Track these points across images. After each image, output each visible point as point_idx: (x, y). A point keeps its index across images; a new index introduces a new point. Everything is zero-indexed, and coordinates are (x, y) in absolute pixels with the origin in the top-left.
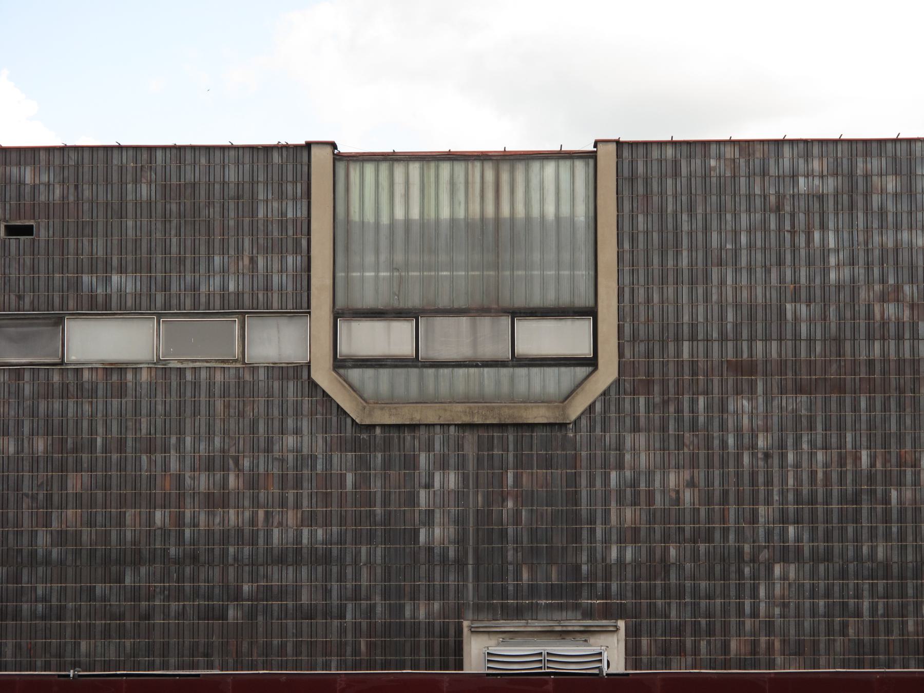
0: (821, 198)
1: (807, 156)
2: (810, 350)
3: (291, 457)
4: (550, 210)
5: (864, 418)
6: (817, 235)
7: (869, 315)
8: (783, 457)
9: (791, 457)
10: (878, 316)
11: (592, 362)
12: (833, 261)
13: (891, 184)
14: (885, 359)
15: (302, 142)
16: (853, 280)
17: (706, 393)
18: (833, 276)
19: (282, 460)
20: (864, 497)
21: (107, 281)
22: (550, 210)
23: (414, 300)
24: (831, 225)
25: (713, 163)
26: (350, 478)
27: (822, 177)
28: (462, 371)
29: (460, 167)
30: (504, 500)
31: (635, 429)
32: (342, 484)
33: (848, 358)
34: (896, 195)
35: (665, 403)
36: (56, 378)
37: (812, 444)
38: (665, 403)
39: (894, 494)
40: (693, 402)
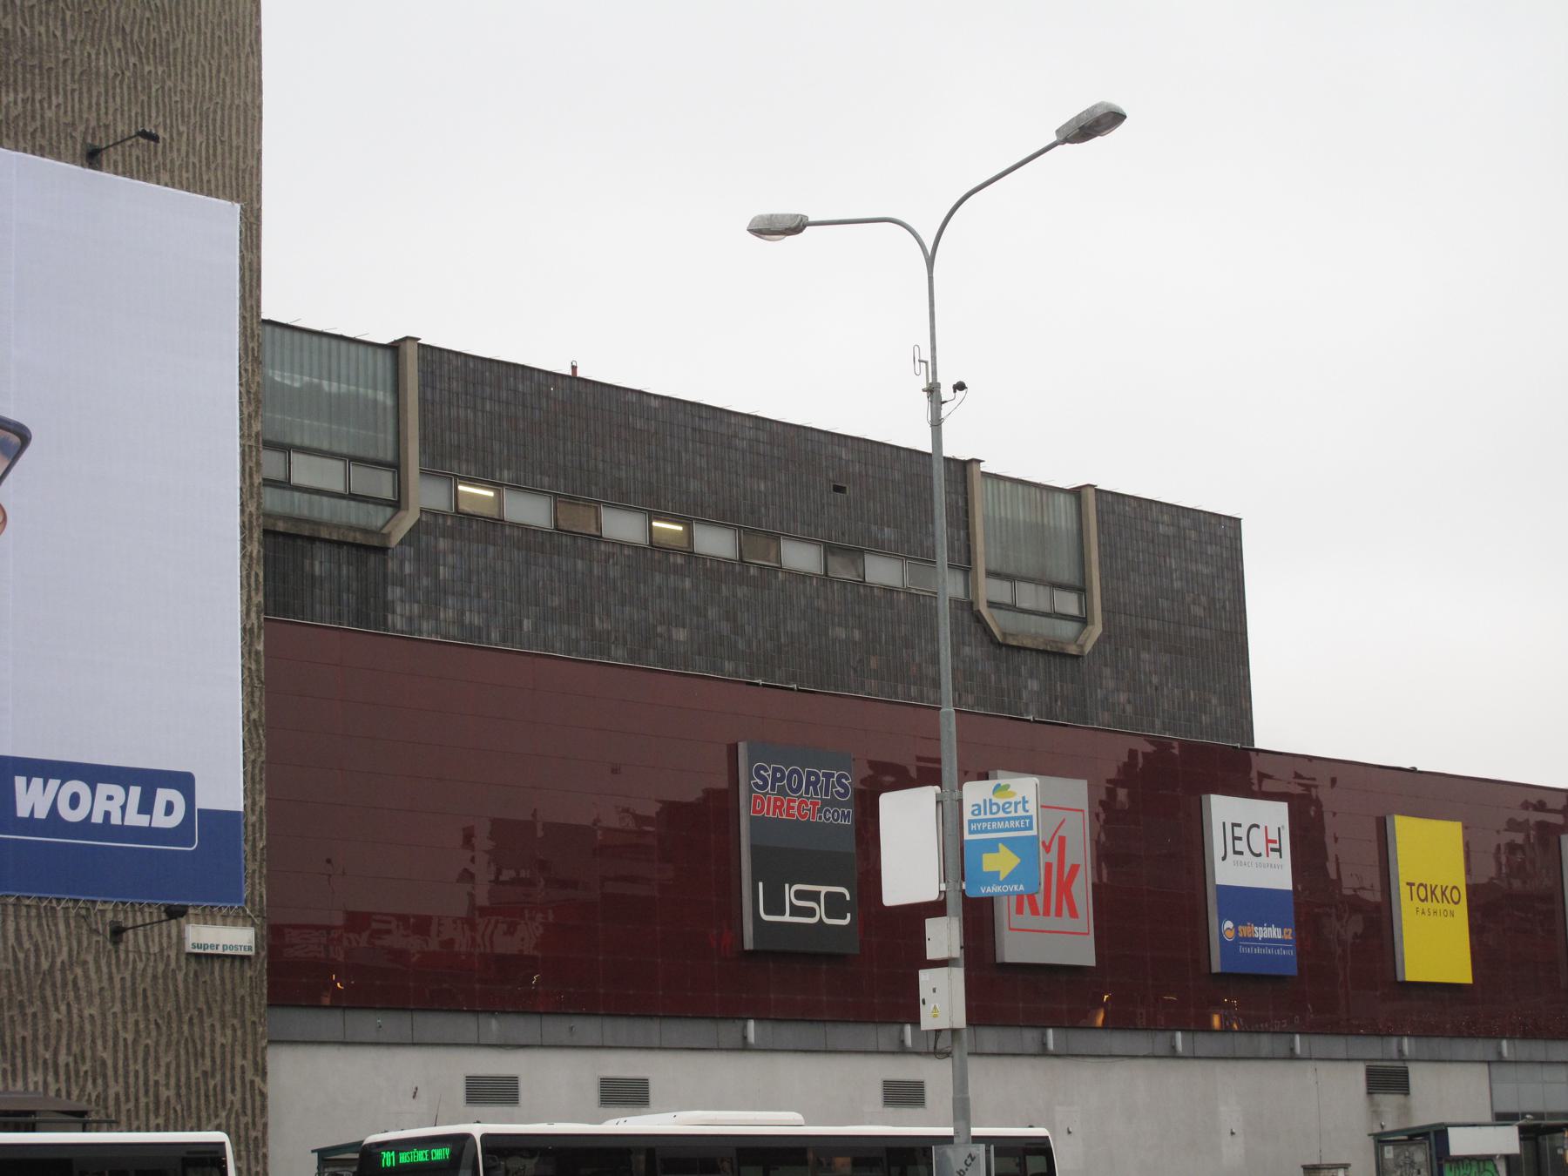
3: (967, 659)
4: (1063, 524)
6: (1168, 560)
11: (1083, 621)
13: (1193, 534)
15: (967, 458)
17: (1132, 647)
19: (964, 662)
21: (882, 530)
22: (1063, 524)
23: (1011, 570)
25: (1127, 508)
26: (993, 676)
27: (1168, 525)
28: (1033, 617)
29: (1026, 488)
30: (1056, 701)
31: (1106, 665)
32: (990, 682)
34: (1195, 541)
35: (1117, 649)
36: (862, 590)
38: (1117, 649)
40: (1127, 651)
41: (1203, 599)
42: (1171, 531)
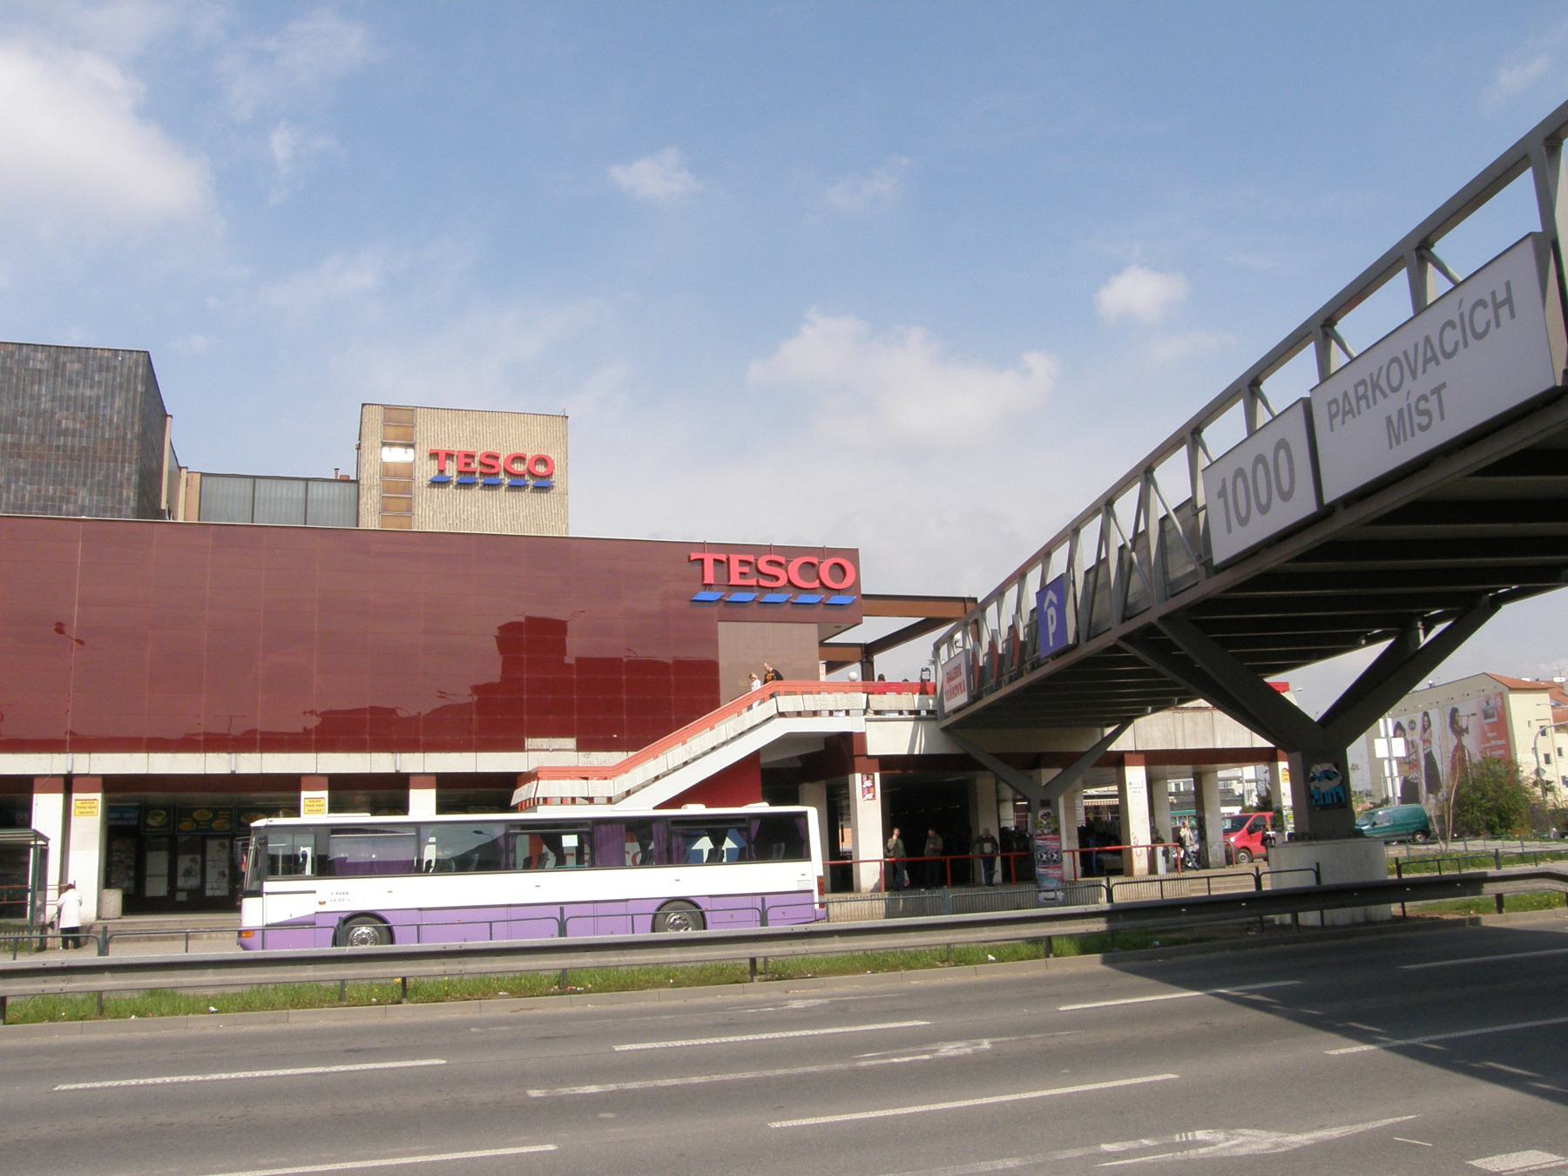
0: (40, 371)
1: (36, 351)
2: (28, 439)
5: (52, 471)
7: (60, 423)
8: (9, 487)
9: (13, 487)
10: (64, 425)
12: (43, 399)
14: (65, 446)
16: (53, 409)
18: (43, 406)
20: (49, 508)
24: (44, 383)
27: (42, 362)
33: (47, 443)
37: (25, 482)
39: (64, 507)
41: (81, 416)
42: (46, 366)
